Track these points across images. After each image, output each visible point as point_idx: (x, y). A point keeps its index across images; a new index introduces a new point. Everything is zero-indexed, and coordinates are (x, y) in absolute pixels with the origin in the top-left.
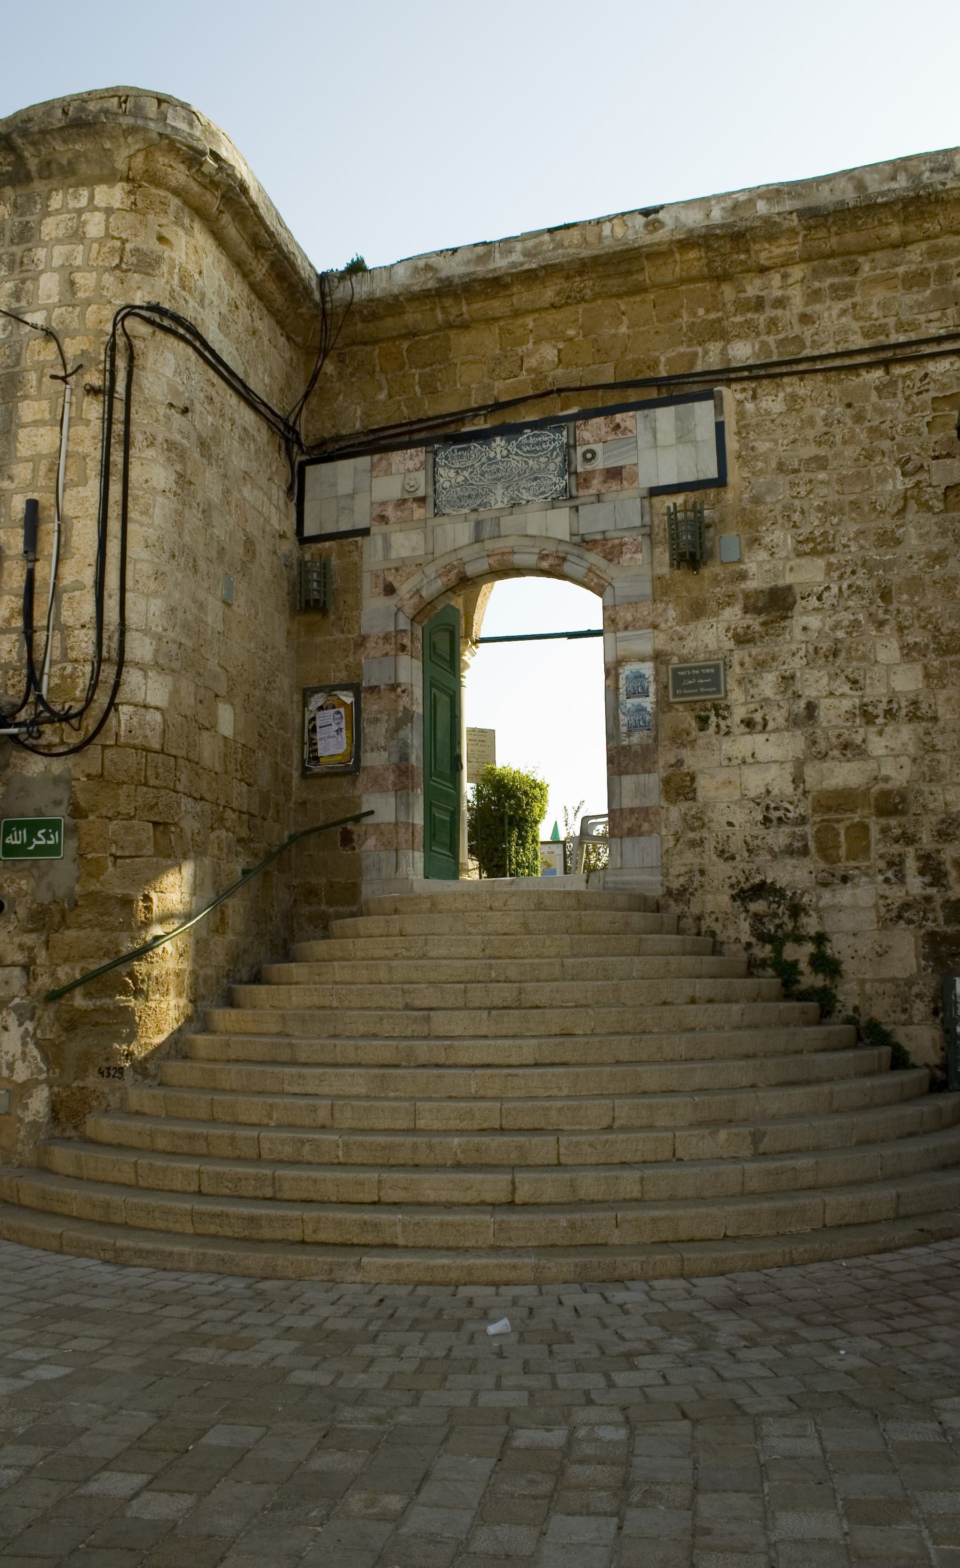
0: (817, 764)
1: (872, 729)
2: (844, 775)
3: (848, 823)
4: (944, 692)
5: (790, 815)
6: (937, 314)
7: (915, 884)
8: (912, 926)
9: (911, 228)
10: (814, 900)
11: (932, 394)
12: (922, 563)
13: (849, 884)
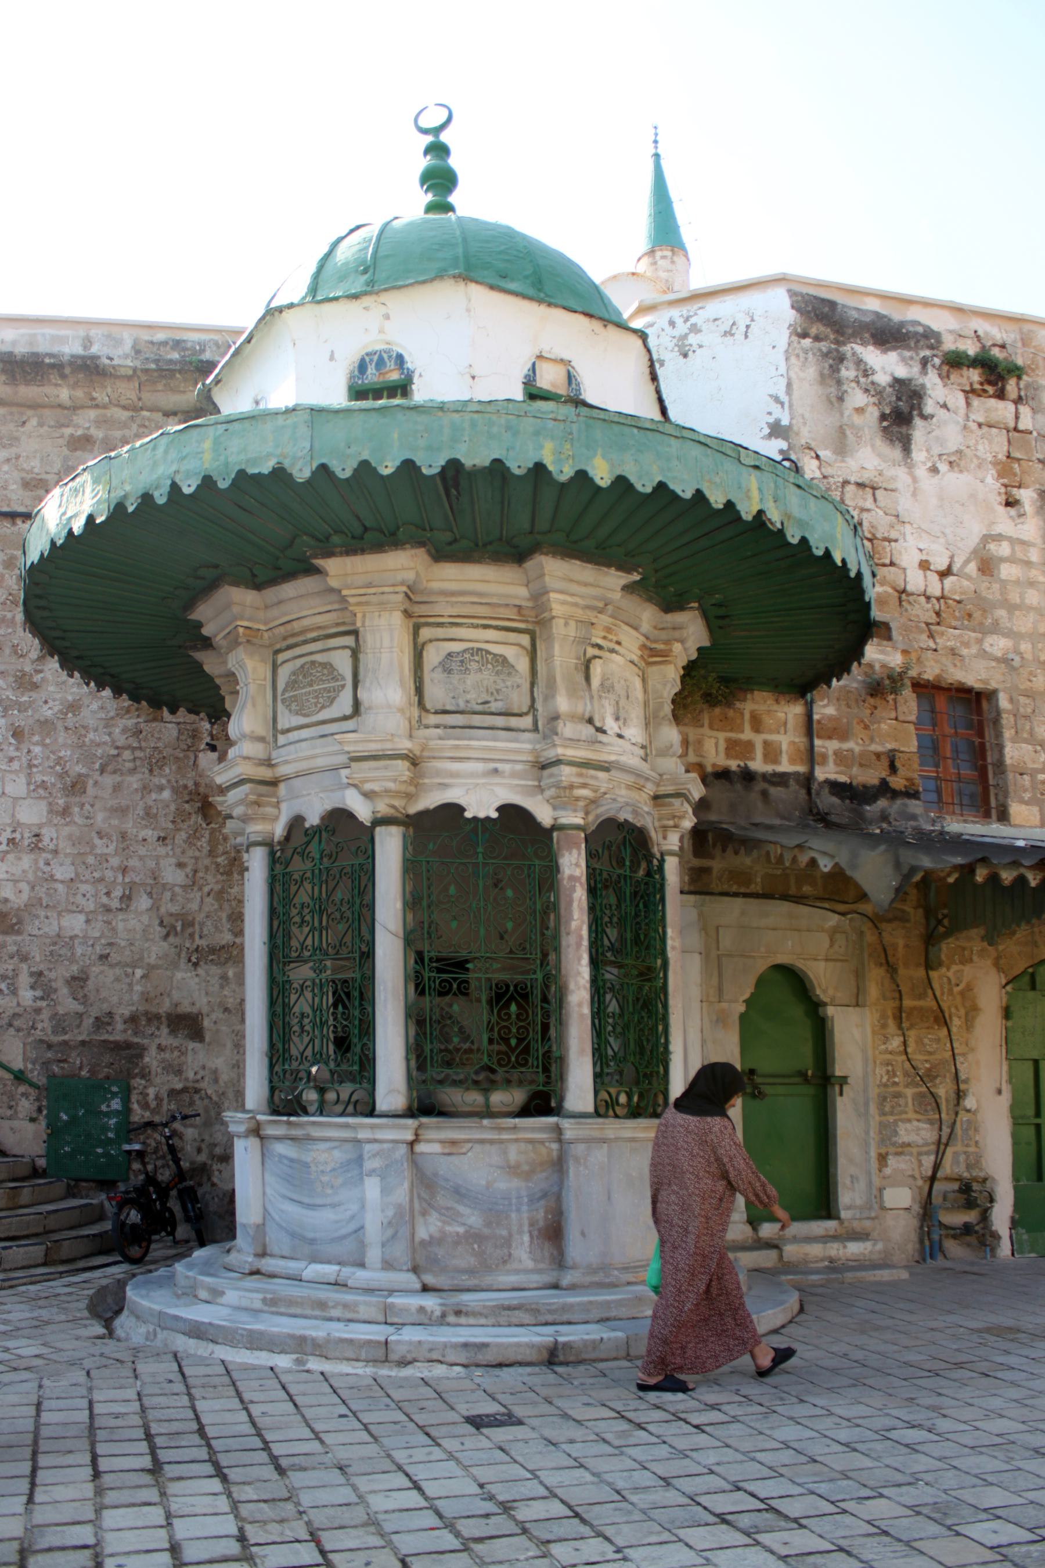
4: (67, 828)
12: (56, 709)
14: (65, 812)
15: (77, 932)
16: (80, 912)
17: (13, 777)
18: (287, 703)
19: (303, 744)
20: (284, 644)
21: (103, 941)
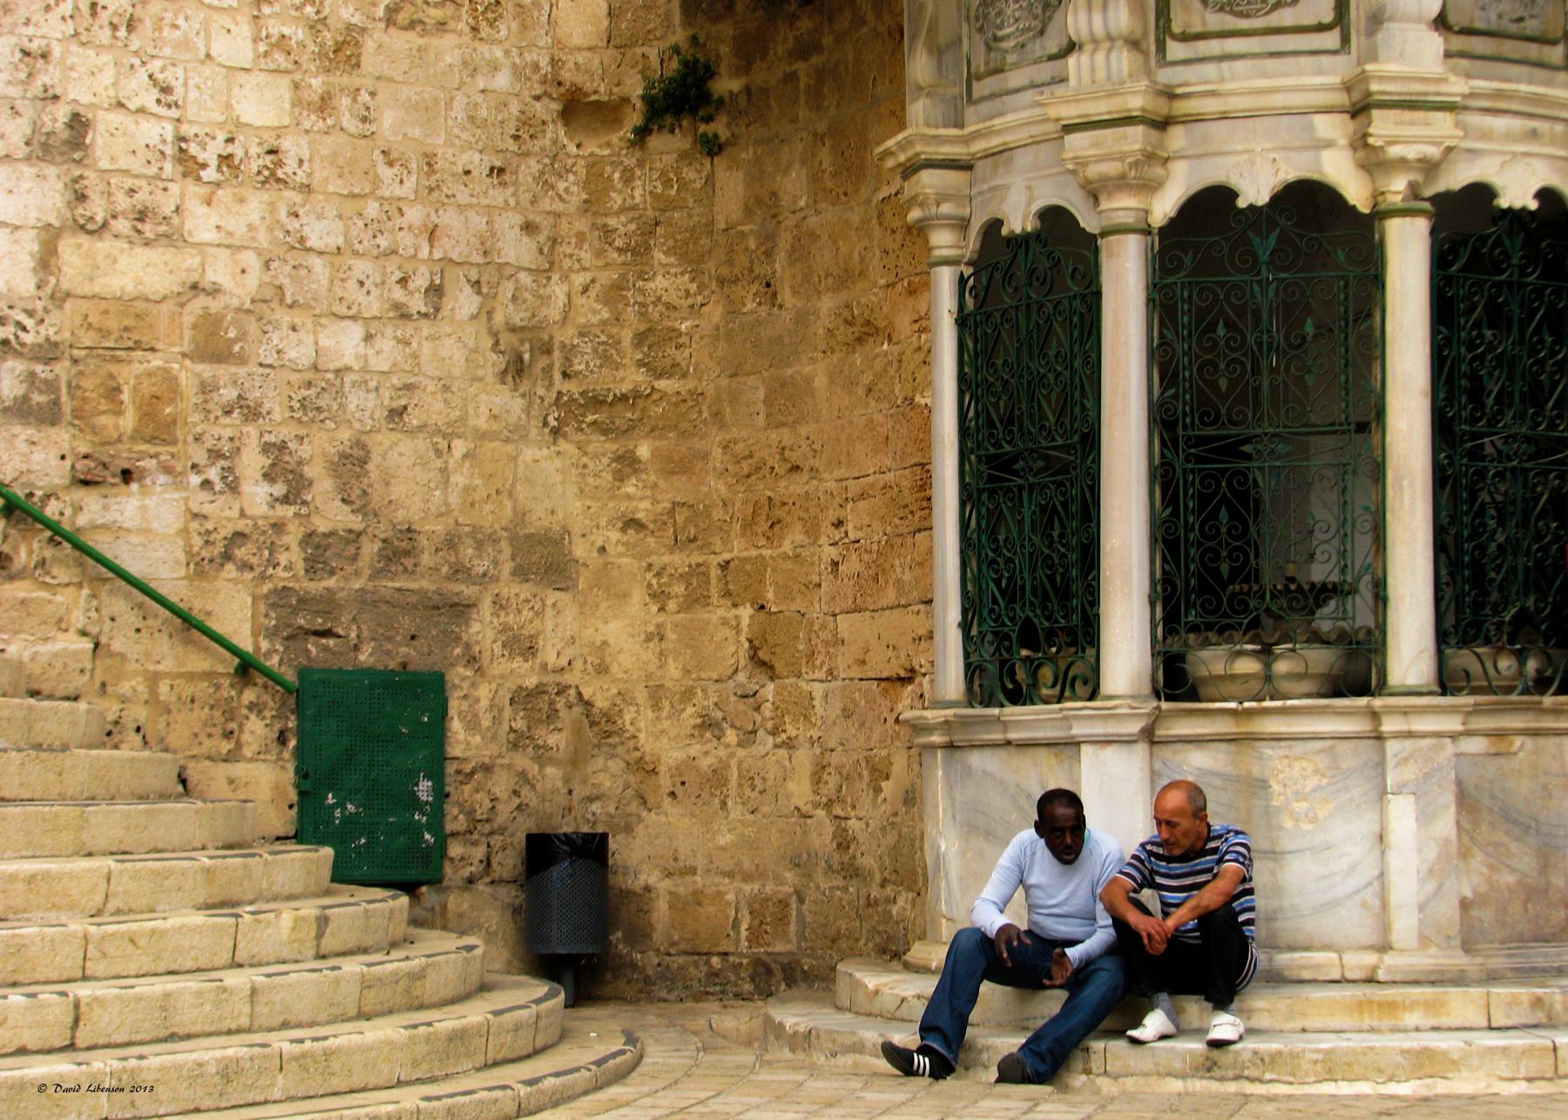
0: (83, 239)
1: (192, 188)
2: (134, 270)
3: (137, 368)
4: (328, 139)
5: (28, 338)
7: (258, 495)
8: (248, 576)
10: (68, 512)
13: (134, 486)
14: (324, 105)
15: (348, 360)
16: (354, 318)
17: (225, 20)
19: (1238, 65)
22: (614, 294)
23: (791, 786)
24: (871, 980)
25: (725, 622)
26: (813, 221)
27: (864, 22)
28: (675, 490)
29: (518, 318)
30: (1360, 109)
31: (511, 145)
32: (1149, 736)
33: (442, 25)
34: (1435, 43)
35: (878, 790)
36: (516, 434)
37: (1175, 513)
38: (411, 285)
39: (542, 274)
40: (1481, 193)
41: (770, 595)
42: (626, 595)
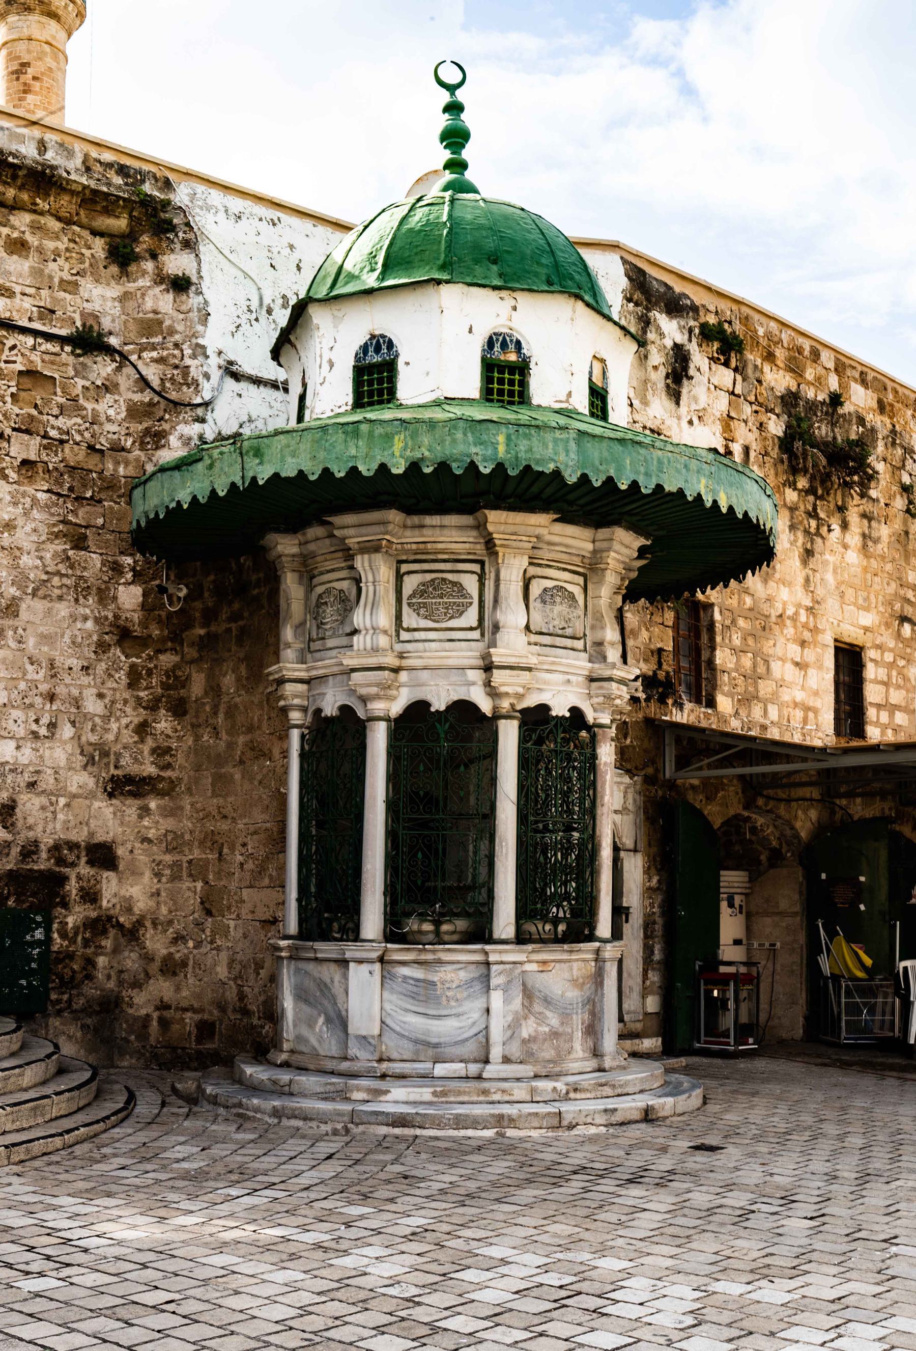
6: (32, 291)
9: (25, 196)
11: (19, 367)
18: (417, 609)
20: (412, 557)
21: (31, 769)
22: (142, 729)
23: (219, 969)
24: (249, 1070)
25: (189, 889)
26: (237, 700)
27: (263, 607)
28: (168, 824)
29: (93, 738)
30: (488, 668)
31: (93, 656)
32: (381, 960)
33: (60, 598)
34: (523, 639)
35: (258, 974)
36: (91, 796)
37: (397, 854)
38: (41, 723)
39: (106, 718)
40: (544, 709)
41: (211, 877)
42: (142, 874)
